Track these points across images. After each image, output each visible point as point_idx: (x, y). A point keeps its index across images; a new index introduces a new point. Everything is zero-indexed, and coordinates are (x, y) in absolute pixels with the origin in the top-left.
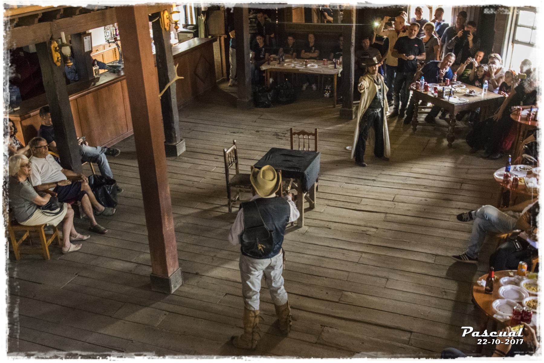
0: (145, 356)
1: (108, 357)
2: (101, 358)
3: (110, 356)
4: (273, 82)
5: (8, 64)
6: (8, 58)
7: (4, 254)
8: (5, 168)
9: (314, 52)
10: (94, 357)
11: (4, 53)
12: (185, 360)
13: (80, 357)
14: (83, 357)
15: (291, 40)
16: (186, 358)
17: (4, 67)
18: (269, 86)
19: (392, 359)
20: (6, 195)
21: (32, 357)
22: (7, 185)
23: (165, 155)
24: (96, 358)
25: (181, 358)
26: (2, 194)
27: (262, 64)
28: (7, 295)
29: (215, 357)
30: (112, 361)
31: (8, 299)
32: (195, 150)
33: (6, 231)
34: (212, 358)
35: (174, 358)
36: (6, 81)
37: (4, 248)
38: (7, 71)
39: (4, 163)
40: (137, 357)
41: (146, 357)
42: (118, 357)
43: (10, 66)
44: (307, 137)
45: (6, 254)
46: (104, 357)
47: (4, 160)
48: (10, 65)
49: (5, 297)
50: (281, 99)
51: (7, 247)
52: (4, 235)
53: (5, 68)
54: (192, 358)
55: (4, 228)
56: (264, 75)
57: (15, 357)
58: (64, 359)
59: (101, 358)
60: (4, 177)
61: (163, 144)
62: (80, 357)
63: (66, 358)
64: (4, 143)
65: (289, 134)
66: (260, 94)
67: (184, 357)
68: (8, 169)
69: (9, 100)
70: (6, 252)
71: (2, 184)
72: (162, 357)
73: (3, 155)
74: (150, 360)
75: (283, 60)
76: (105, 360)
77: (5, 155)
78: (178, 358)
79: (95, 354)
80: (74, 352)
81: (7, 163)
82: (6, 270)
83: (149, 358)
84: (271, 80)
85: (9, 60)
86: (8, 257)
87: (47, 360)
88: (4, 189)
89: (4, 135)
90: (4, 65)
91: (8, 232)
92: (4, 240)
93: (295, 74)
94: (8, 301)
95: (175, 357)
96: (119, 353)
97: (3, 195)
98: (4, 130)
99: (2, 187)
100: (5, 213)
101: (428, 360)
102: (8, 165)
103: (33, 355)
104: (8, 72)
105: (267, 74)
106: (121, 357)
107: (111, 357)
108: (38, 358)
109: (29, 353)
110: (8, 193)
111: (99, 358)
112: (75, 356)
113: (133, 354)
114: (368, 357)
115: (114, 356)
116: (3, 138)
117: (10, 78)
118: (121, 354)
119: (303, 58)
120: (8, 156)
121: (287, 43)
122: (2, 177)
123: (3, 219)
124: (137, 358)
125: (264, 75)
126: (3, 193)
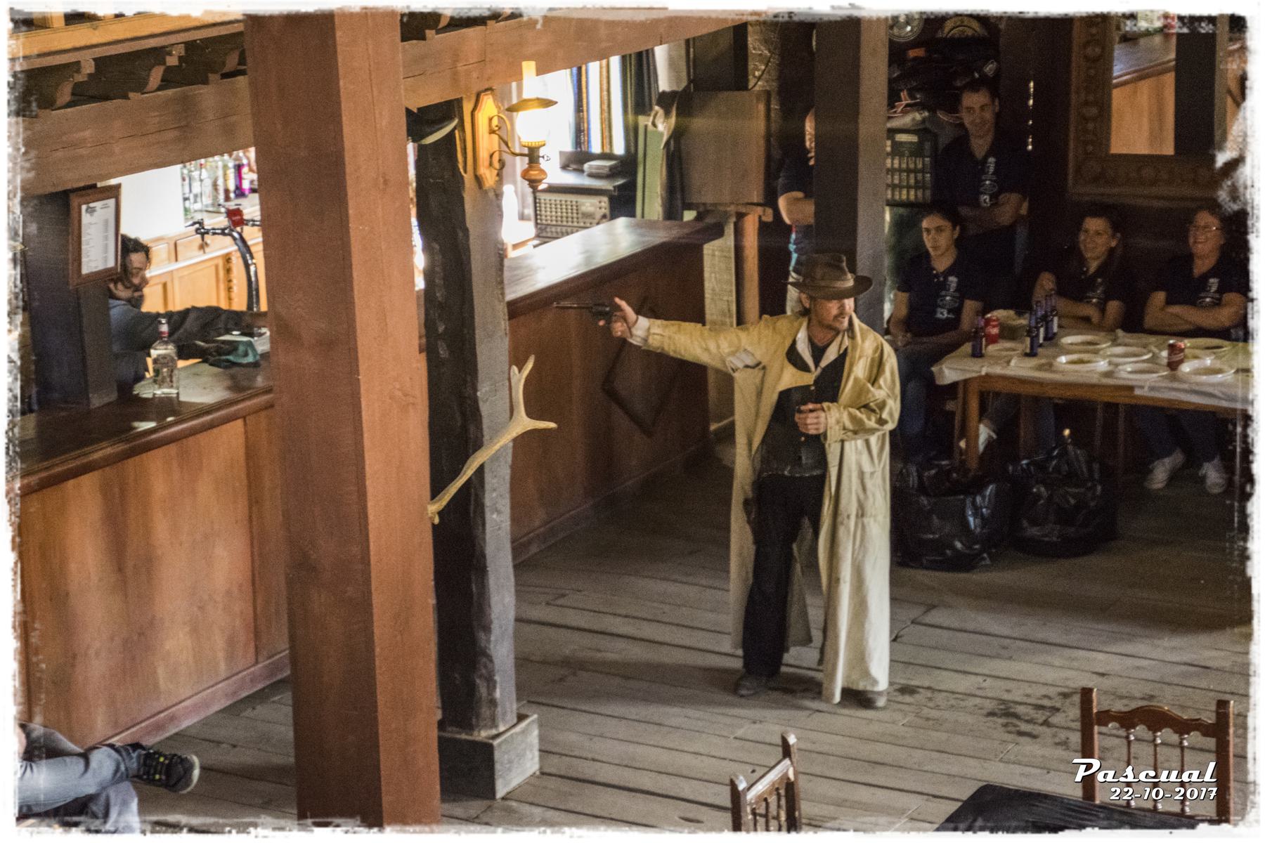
0: (338, 826)
1: (252, 829)
2: (234, 831)
3: (255, 825)
4: (990, 444)
5: (19, 149)
6: (18, 134)
7: (11, 589)
8: (10, 390)
9: (1217, 303)
10: (217, 830)
11: (10, 124)
12: (430, 836)
13: (185, 830)
14: (192, 830)
15: (1096, 238)
16: (432, 832)
17: (9, 155)
18: (973, 464)
19: (913, 834)
20: (15, 452)
21: (74, 829)
22: (16, 430)
23: (438, 796)
24: (223, 832)
25: (421, 832)
26: (3, 451)
27: (940, 354)
28: (17, 684)
29: (500, 830)
30: (260, 839)
31: (20, 694)
32: (588, 770)
33: (13, 541)
34: (494, 832)
35: (405, 832)
36: (15, 188)
37: (10, 575)
38: (15, 164)
39: (10, 380)
40: (318, 830)
41: (338, 829)
42: (274, 829)
43: (24, 154)
44: (1175, 738)
45: (15, 591)
46: (243, 829)
47: (10, 372)
48: (23, 150)
49: (11, 690)
50: (1034, 531)
51: (15, 573)
52: (9, 545)
53: (12, 159)
54: (448, 831)
55: (10, 529)
56: (950, 406)
57: (35, 829)
58: (148, 835)
59: (234, 831)
60: (10, 411)
61: (434, 733)
62: (185, 830)
63: (152, 832)
64: (10, 331)
65: (1075, 712)
66: (924, 500)
67: (427, 829)
68: (18, 392)
69: (21, 232)
70: (14, 586)
71: (6, 427)
72: (376, 829)
73: (6, 359)
74: (350, 836)
75: (1050, 337)
76: (243, 836)
77: (11, 361)
78: (415, 832)
79: (221, 821)
80: (171, 818)
81: (16, 379)
82: (14, 627)
83: (346, 832)
84: (984, 433)
85: (20, 140)
86: (19, 597)
87: (109, 835)
88: (10, 440)
89: (10, 314)
90: (10, 150)
91: (18, 540)
92: (10, 557)
93: (1111, 407)
94: (20, 700)
95: (407, 828)
96: (276, 821)
97: (7, 453)
98: (10, 302)
99: (4, 435)
100: (12, 495)
101: (994, 835)
102: (19, 383)
103: (76, 824)
104: (18, 167)
105: (965, 403)
106: (282, 829)
107: (259, 829)
108: (89, 831)
109: (68, 819)
110: (18, 449)
111: (230, 832)
112: (175, 828)
113: (309, 821)
114: (856, 830)
115: (264, 826)
116: (7, 319)
117: (22, 181)
118: (282, 822)
119: (1152, 332)
120: (19, 363)
121: (1075, 253)
122: (5, 412)
123: (7, 508)
124: (319, 831)
125: (950, 406)
126: (8, 448)
